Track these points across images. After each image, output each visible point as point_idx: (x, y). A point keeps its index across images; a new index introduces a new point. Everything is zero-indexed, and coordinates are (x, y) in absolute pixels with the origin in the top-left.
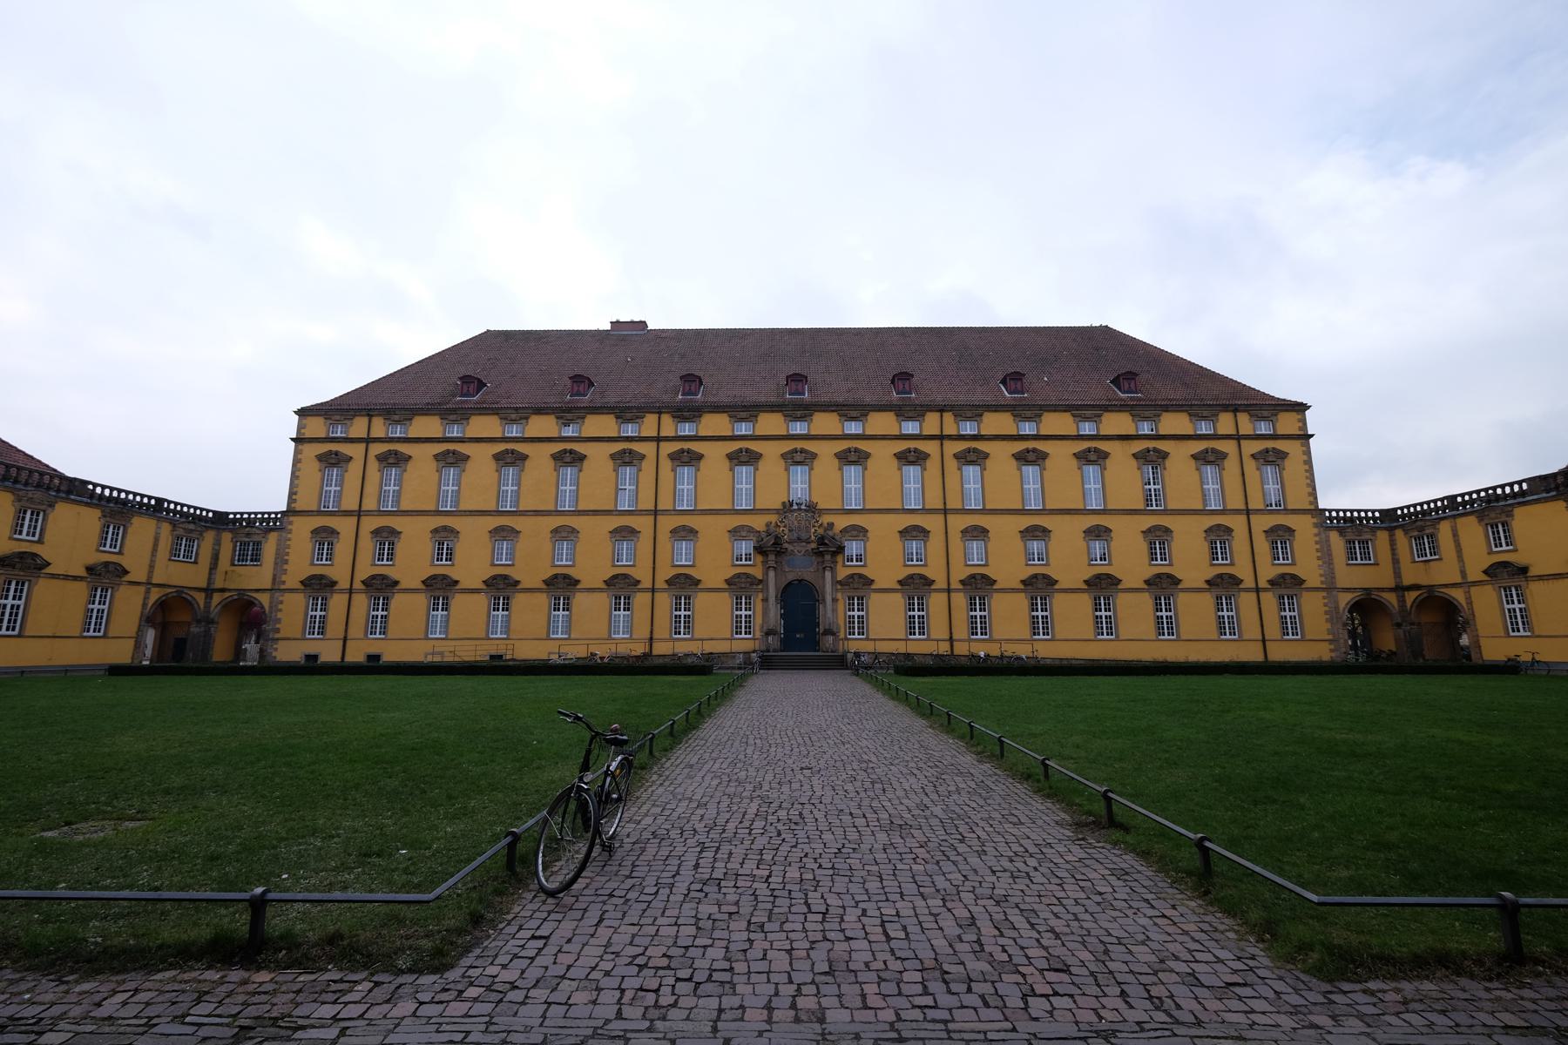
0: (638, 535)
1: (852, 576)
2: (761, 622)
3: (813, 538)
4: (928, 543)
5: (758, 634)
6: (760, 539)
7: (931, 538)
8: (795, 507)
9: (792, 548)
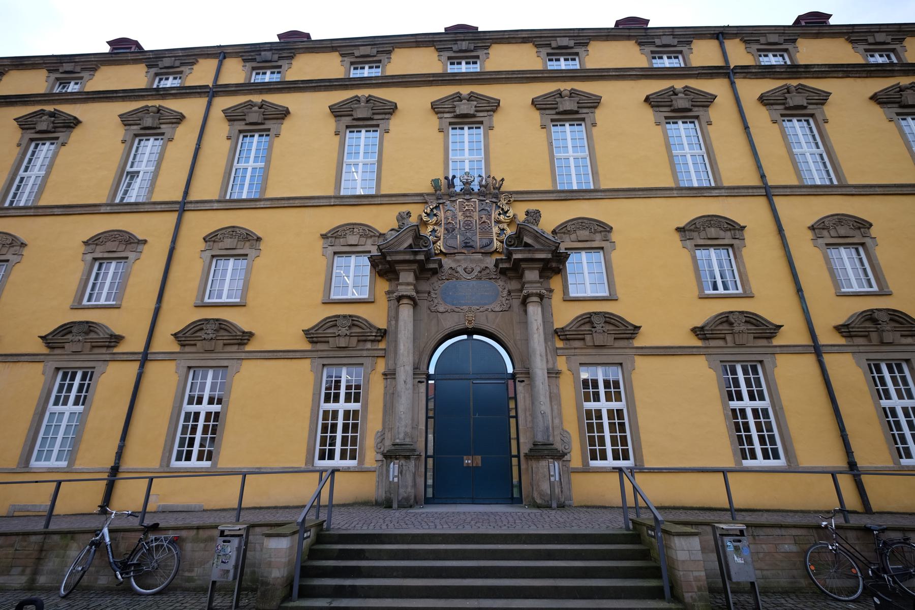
0: (140, 247)
1: (588, 319)
2: (379, 427)
3: (496, 244)
4: (745, 252)
5: (371, 458)
7: (747, 241)
9: (454, 265)
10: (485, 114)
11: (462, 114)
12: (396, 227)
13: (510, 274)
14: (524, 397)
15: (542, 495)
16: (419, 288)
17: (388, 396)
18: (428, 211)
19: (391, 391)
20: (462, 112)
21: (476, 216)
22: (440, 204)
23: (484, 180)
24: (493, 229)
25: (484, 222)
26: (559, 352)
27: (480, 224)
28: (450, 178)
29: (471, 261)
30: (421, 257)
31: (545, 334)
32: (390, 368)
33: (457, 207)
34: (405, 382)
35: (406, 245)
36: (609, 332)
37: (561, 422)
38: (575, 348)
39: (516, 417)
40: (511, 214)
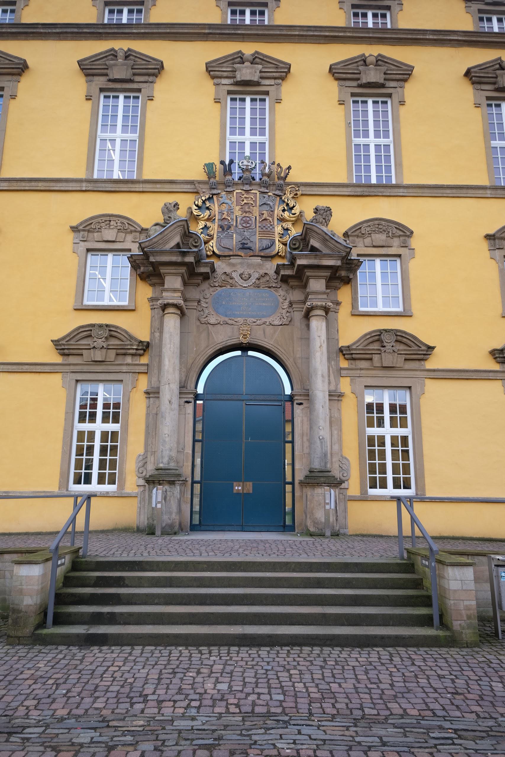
2: (141, 450)
3: (278, 247)
9: (228, 270)
10: (272, 82)
11: (242, 81)
12: (161, 221)
13: (293, 282)
14: (302, 422)
15: (315, 523)
16: (188, 296)
17: (151, 416)
18: (200, 203)
19: (154, 412)
20: (244, 78)
21: (256, 211)
22: (213, 195)
23: (267, 168)
24: (276, 228)
25: (265, 219)
26: (344, 372)
27: (260, 222)
28: (227, 162)
29: (249, 266)
30: (190, 259)
31: (328, 352)
32: (153, 386)
33: (234, 199)
34: (170, 402)
35: (173, 243)
36: (399, 352)
37: (341, 449)
38: (361, 369)
39: (292, 442)
40: (296, 210)
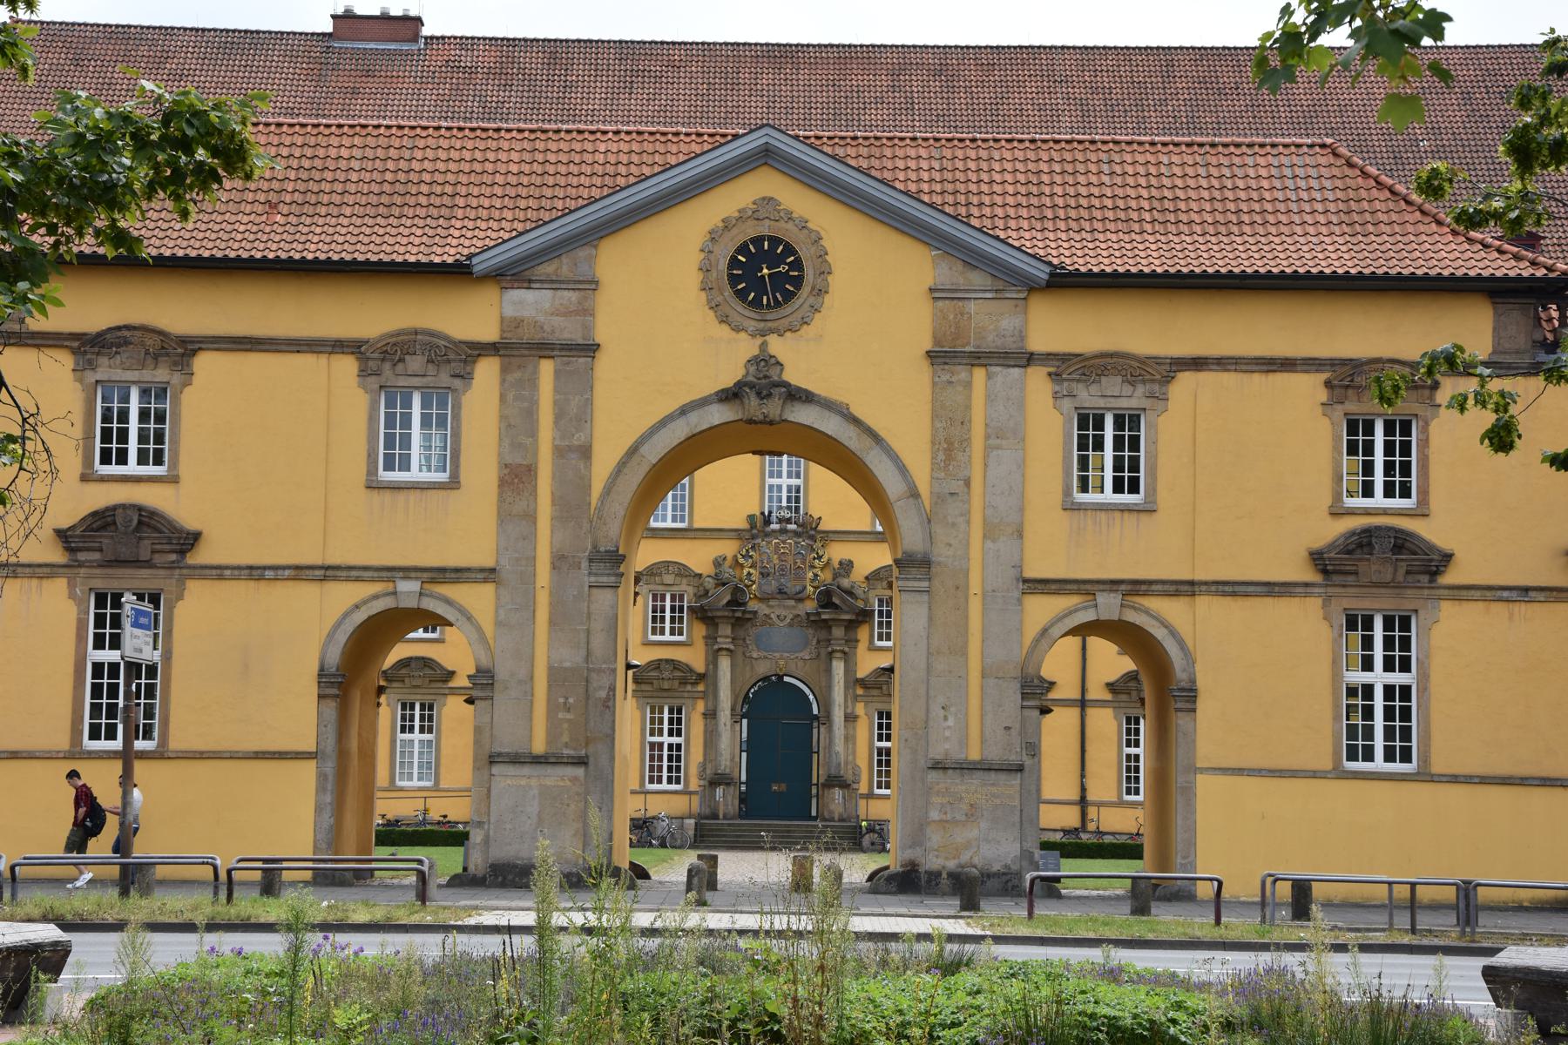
2: (701, 759)
3: (810, 589)
5: (694, 784)
6: (702, 593)
8: (775, 526)
9: (767, 612)
12: (713, 575)
15: (831, 812)
18: (744, 552)
21: (790, 559)
26: (859, 698)
31: (845, 682)
35: (725, 601)
37: (854, 759)
39: (818, 753)
40: (825, 559)
